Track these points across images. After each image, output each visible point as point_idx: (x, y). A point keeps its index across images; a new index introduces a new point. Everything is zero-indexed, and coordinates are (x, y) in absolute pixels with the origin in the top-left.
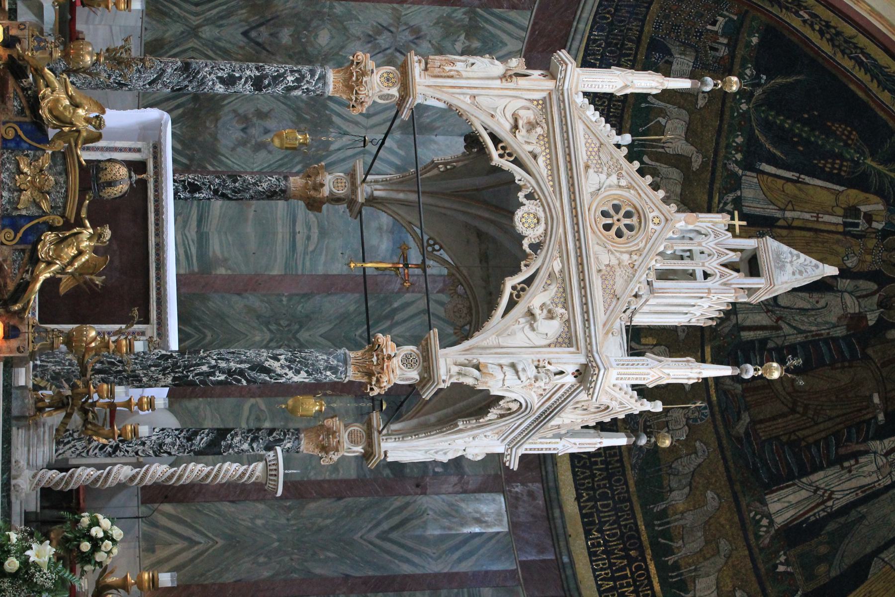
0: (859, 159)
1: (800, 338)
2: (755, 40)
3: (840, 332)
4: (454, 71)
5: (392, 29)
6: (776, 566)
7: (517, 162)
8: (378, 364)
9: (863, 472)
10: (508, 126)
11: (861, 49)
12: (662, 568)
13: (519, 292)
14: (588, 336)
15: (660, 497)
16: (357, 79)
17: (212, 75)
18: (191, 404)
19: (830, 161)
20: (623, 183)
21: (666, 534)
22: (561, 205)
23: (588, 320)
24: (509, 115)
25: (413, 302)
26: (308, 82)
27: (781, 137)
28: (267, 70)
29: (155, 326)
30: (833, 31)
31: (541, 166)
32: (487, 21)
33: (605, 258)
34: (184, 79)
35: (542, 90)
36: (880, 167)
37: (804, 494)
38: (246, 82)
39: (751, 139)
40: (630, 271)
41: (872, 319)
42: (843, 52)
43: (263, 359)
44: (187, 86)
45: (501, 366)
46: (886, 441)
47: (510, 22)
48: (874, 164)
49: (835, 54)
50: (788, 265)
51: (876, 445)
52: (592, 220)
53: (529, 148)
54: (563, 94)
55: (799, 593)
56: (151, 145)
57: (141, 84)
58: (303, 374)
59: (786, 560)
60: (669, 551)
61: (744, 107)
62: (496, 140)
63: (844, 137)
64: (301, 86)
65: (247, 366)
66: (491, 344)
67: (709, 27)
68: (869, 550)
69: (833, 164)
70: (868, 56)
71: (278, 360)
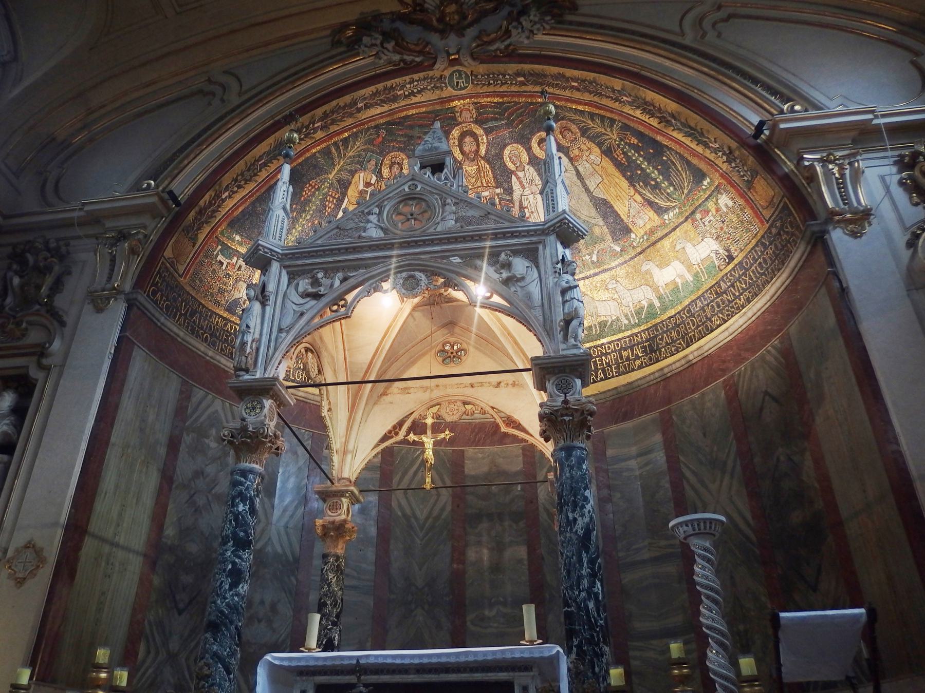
0: (328, 183)
2: (238, 238)
4: (252, 343)
5: (192, 492)
6: (593, 262)
8: (572, 415)
9: (533, 203)
10: (313, 302)
11: (255, 161)
14: (528, 233)
16: (250, 437)
17: (228, 595)
19: (327, 203)
20: (377, 210)
23: (512, 233)
24: (302, 301)
25: (398, 500)
26: (247, 489)
28: (229, 532)
29: (517, 674)
30: (239, 177)
32: (196, 420)
34: (228, 629)
35: (280, 272)
36: (336, 169)
38: (240, 557)
40: (461, 205)
42: (256, 175)
43: (574, 537)
44: (236, 628)
45: (564, 302)
46: (514, 188)
47: (200, 403)
48: (333, 174)
49: (256, 181)
50: (434, 145)
53: (337, 283)
54: (286, 255)
55: (612, 245)
56: (298, 678)
57: (227, 684)
58: (587, 493)
59: (590, 254)
63: (313, 190)
64: (250, 496)
65: (584, 555)
66: (541, 313)
67: (224, 267)
68: (587, 199)
69: (329, 201)
70: (261, 158)
71: (575, 520)
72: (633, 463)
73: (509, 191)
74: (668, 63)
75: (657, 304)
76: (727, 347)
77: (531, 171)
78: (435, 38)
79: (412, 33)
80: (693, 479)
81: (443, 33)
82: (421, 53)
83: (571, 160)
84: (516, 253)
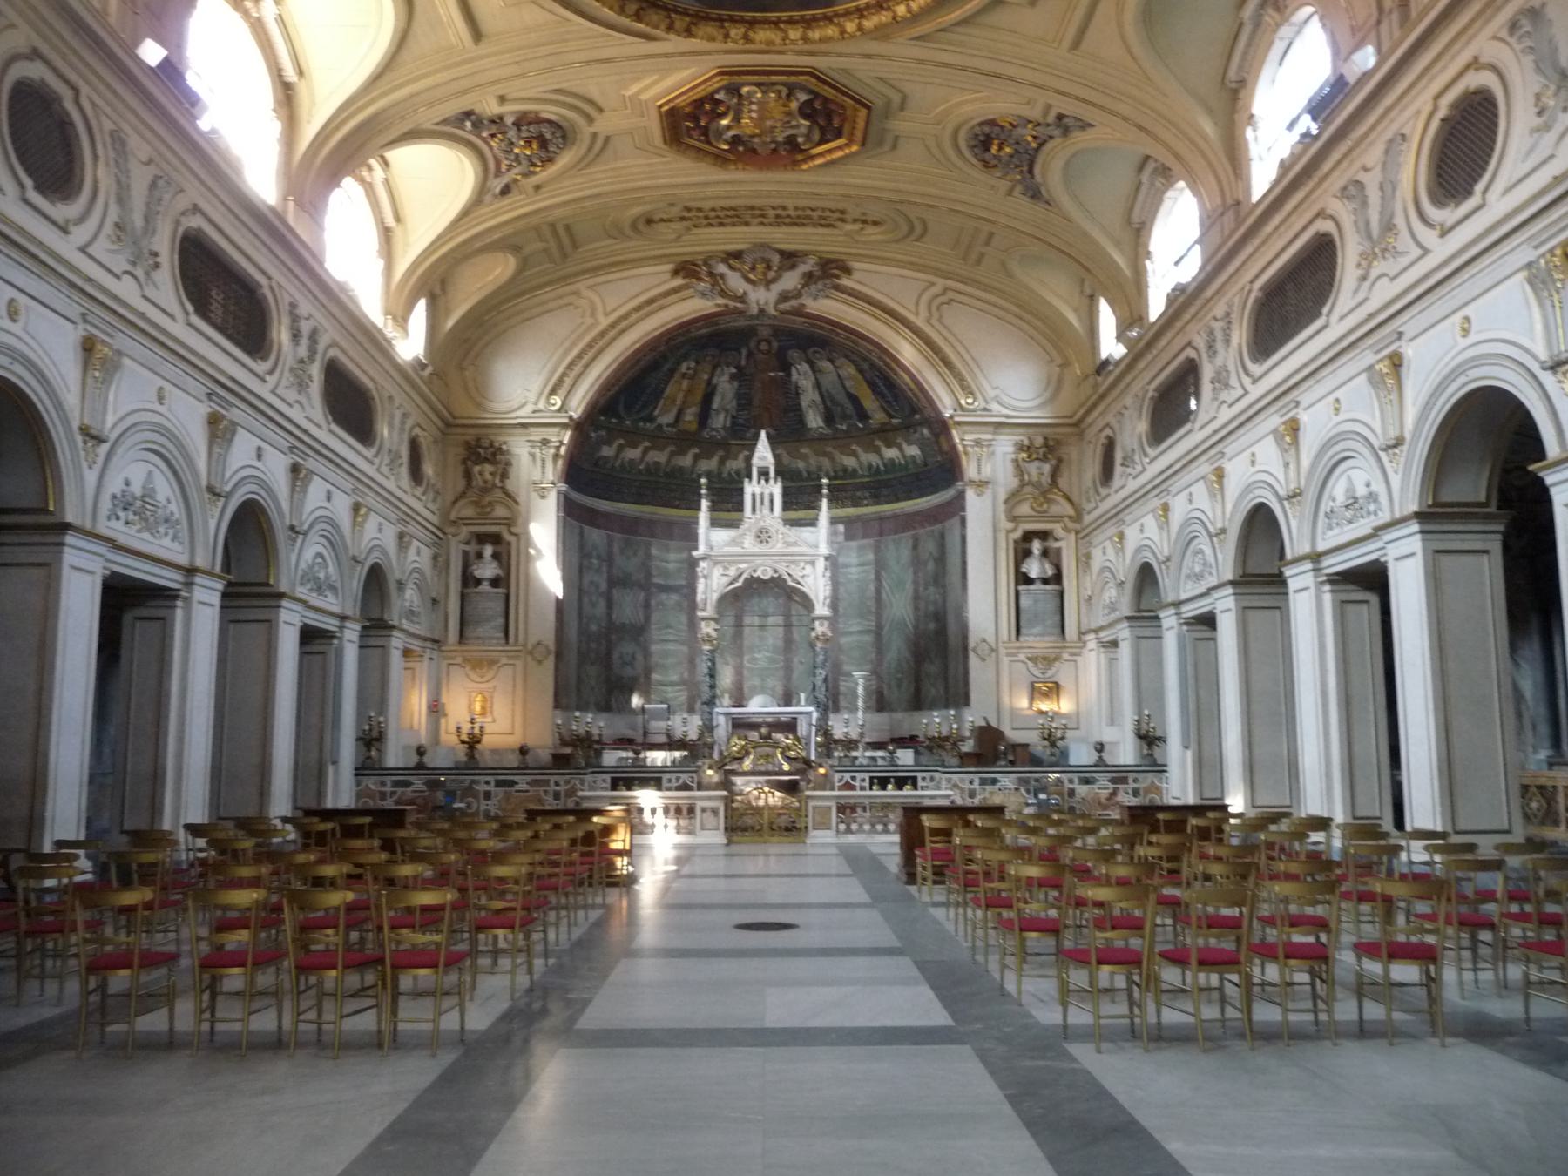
1: (734, 403)
3: (736, 384)
7: (740, 575)
12: (835, 478)
13: (794, 580)
18: (746, 690)
22: (759, 560)
31: (743, 566)
33: (780, 545)
37: (811, 412)
51: (795, 377)
52: (764, 548)
62: (731, 583)
73: (789, 375)
77: (805, 367)
78: (748, 287)
80: (887, 588)
83: (836, 367)
84: (807, 562)
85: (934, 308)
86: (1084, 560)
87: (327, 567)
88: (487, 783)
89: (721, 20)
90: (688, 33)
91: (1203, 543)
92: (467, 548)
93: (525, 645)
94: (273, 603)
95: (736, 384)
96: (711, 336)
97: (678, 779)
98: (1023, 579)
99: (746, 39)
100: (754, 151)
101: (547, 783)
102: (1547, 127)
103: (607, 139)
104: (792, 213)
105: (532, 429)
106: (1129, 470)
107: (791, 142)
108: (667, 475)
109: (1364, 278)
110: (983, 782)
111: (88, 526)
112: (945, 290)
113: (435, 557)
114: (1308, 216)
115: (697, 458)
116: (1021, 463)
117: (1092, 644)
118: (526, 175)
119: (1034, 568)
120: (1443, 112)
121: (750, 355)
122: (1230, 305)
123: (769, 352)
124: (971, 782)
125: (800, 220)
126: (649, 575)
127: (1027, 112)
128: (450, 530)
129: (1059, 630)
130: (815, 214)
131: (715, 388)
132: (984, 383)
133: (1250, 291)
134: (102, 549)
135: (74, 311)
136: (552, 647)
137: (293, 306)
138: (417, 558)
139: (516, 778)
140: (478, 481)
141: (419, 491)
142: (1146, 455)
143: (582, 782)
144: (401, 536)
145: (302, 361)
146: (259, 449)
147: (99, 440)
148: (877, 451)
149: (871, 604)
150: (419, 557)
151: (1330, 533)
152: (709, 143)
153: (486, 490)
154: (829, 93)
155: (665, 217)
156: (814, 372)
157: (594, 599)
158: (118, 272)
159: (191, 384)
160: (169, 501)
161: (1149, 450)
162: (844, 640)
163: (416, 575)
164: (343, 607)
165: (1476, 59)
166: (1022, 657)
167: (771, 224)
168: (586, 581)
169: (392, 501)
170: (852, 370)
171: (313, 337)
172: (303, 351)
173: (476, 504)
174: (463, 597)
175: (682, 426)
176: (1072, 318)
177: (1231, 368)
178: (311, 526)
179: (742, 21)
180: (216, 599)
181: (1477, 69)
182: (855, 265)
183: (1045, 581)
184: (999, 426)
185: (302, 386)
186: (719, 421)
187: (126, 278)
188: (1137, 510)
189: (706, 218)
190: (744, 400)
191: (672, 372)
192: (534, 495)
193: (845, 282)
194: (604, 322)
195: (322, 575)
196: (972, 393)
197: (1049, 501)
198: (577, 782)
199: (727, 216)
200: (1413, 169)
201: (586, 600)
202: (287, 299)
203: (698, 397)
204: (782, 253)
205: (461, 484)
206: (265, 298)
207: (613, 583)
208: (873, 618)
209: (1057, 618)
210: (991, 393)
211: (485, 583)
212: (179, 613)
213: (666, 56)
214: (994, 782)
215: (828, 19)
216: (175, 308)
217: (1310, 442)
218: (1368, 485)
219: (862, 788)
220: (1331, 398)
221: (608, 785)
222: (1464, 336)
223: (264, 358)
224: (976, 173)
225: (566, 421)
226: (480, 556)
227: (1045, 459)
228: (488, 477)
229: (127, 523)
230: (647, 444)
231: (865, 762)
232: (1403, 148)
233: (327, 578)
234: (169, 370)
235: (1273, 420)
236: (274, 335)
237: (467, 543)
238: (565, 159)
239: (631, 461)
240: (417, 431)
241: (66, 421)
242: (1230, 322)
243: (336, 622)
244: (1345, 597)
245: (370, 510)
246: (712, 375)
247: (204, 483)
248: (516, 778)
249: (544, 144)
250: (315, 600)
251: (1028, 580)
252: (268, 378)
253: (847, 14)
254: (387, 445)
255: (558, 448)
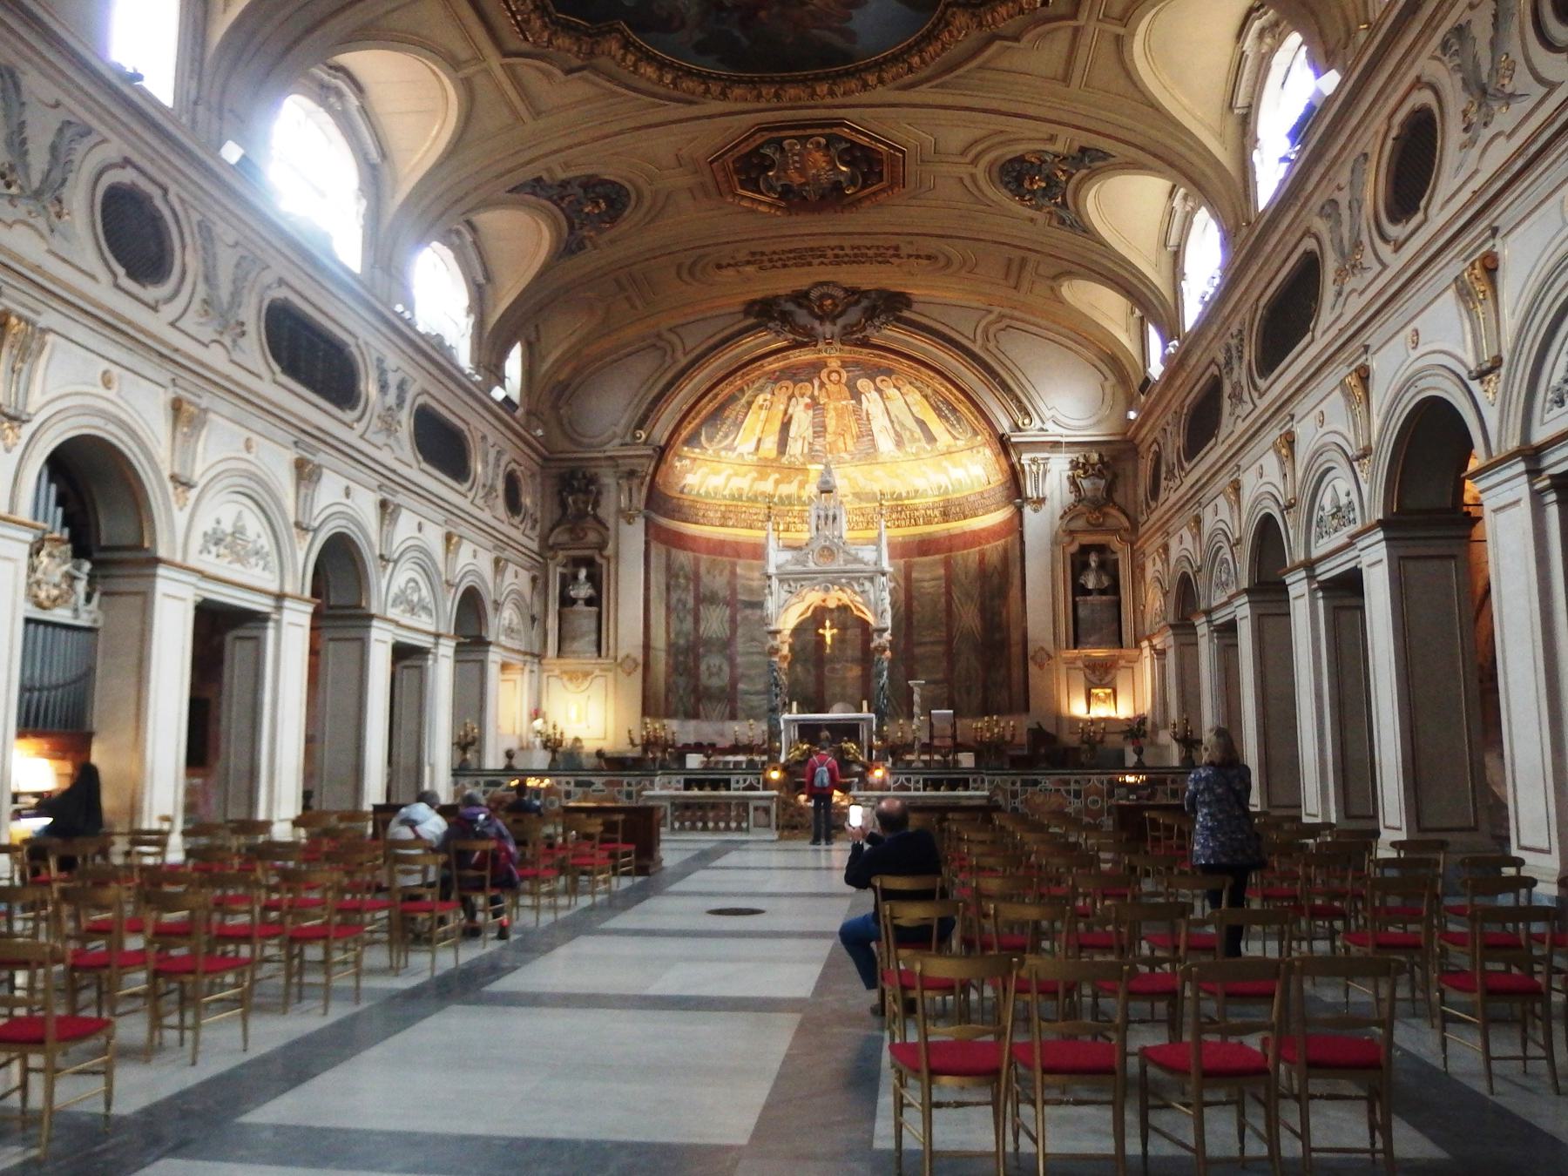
1: (811, 429)
2: (686, 449)
12: (908, 498)
15: (875, 494)
18: (827, 698)
21: (892, 494)
27: (726, 436)
39: (725, 448)
41: (808, 400)
60: (900, 494)
61: (710, 452)
72: (926, 584)
73: (860, 402)
74: (963, 368)
75: (950, 488)
76: (983, 530)
77: (875, 395)
78: (816, 324)
79: (802, 317)
81: (821, 319)
82: (809, 336)
84: (865, 578)
85: (991, 336)
86: (1138, 570)
87: (420, 590)
88: (568, 783)
89: (751, 81)
90: (724, 96)
91: (1226, 553)
92: (564, 571)
93: (616, 659)
94: (365, 623)
95: (811, 412)
96: (782, 370)
97: (745, 781)
98: (1079, 590)
99: (777, 96)
100: (805, 198)
101: (620, 784)
102: (1472, 142)
103: (668, 197)
104: (848, 251)
105: (620, 461)
106: (1171, 484)
107: (837, 187)
108: (749, 499)
109: (1339, 294)
110: (1024, 783)
111: (178, 559)
112: (1002, 317)
113: (534, 579)
114: (1298, 234)
115: (777, 483)
116: (1078, 481)
117: (1147, 652)
118: (600, 231)
119: (1091, 582)
120: (1394, 133)
121: (822, 385)
122: (1242, 323)
123: (839, 381)
124: (1013, 783)
125: (858, 258)
126: (734, 592)
127: (1049, 147)
128: (550, 554)
129: (1116, 638)
130: (870, 253)
131: (791, 417)
132: (1041, 404)
133: (1256, 309)
134: (193, 579)
135: (164, 378)
136: (640, 659)
137: (380, 361)
138: (515, 581)
139: (593, 779)
140: (571, 510)
141: (517, 520)
142: (1183, 469)
143: (652, 783)
144: (497, 561)
145: (390, 409)
146: (347, 488)
147: (188, 485)
148: (945, 471)
149: (942, 615)
150: (517, 580)
151: (1321, 542)
152: (761, 193)
153: (582, 515)
154: (864, 141)
155: (732, 262)
156: (881, 396)
157: (681, 615)
158: (206, 342)
159: (279, 434)
160: (259, 536)
161: (1186, 465)
162: (918, 651)
163: (513, 596)
164: (437, 627)
165: (1418, 78)
166: (1080, 664)
167: (831, 263)
168: (674, 597)
169: (484, 528)
170: (918, 396)
171: (401, 387)
172: (391, 399)
173: (571, 531)
174: (561, 618)
175: (763, 452)
176: (1124, 338)
177: (1244, 382)
178: (401, 555)
179: (772, 82)
180: (306, 621)
181: (1419, 89)
182: (914, 298)
183: (1102, 592)
184: (1055, 445)
185: (389, 428)
186: (795, 448)
187: (214, 345)
188: (1176, 522)
189: (771, 261)
190: (820, 430)
191: (750, 404)
192: (622, 522)
193: (906, 314)
194: (684, 361)
195: (415, 598)
196: (1028, 414)
197: (1105, 515)
198: (647, 783)
199: (789, 259)
200: (1373, 188)
201: (674, 616)
202: (375, 355)
203: (777, 425)
204: (846, 290)
205: (557, 513)
206: (351, 353)
207: (699, 600)
208: (944, 629)
209: (1116, 625)
210: (1047, 414)
211: (581, 602)
212: (271, 634)
213: (710, 117)
214: (1036, 783)
215: (848, 73)
216: (261, 368)
217: (1303, 451)
218: (1348, 494)
219: (917, 789)
220: (1316, 411)
221: (681, 785)
222: (1414, 348)
223: (353, 407)
224: (1015, 206)
225: (650, 452)
226: (575, 578)
227: (1100, 475)
228: (581, 506)
229: (218, 556)
230: (730, 471)
231: (921, 765)
232: (1367, 166)
233: (420, 600)
234: (259, 425)
235: (1273, 434)
236: (362, 386)
237: (565, 566)
238: (631, 217)
239: (716, 488)
240: (513, 466)
241: (157, 471)
242: (1242, 340)
243: (431, 640)
244: (1337, 603)
245: (461, 537)
246: (788, 405)
247: (292, 520)
248: (593, 779)
249: (611, 203)
250: (406, 620)
251: (1089, 592)
252: (355, 425)
253: (868, 68)
254: (480, 480)
255: (644, 477)
